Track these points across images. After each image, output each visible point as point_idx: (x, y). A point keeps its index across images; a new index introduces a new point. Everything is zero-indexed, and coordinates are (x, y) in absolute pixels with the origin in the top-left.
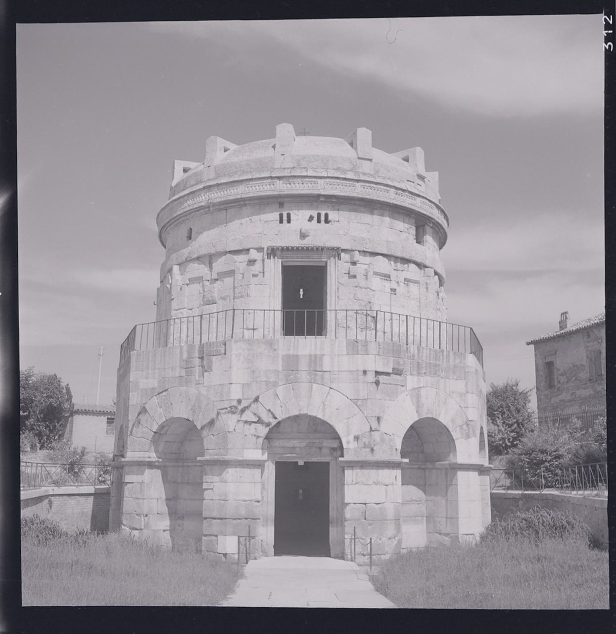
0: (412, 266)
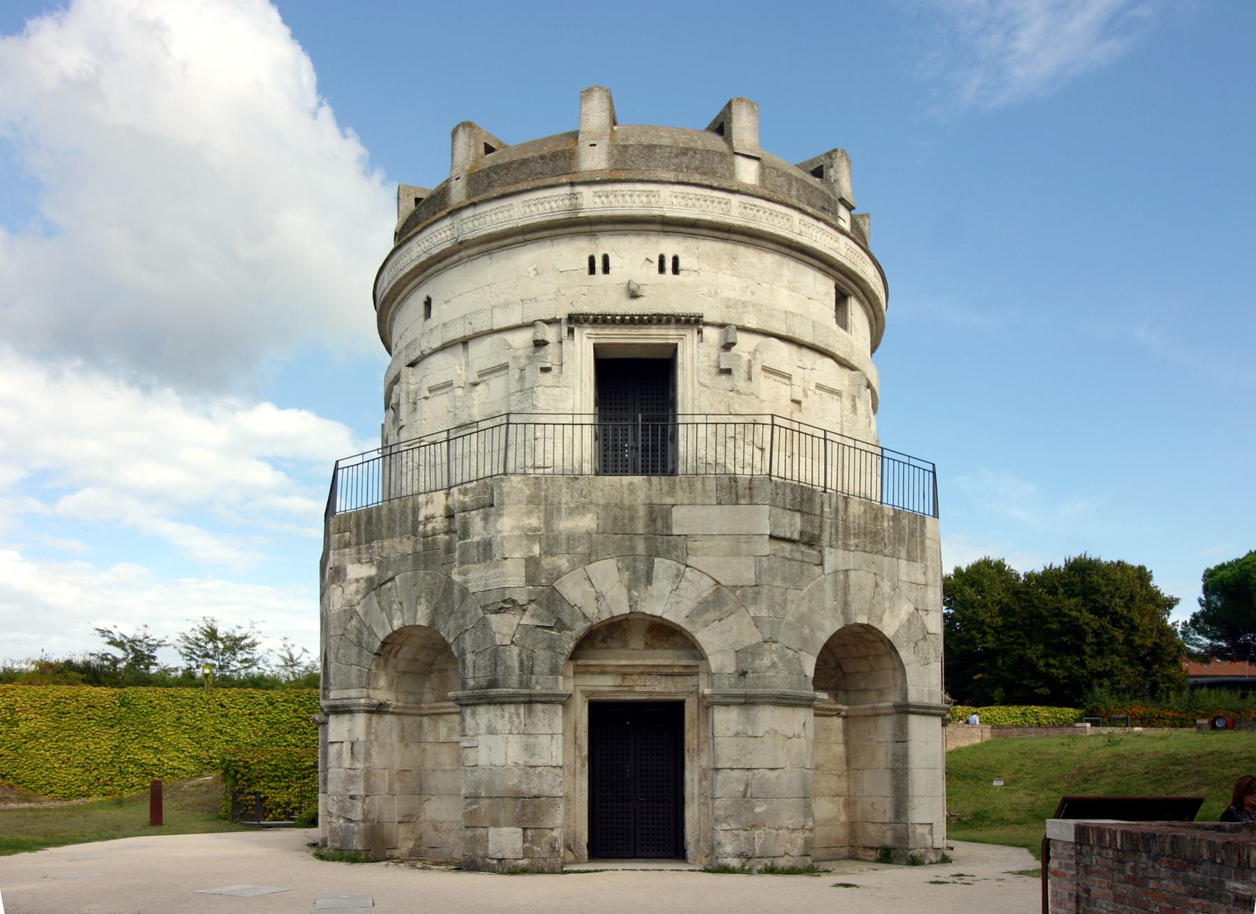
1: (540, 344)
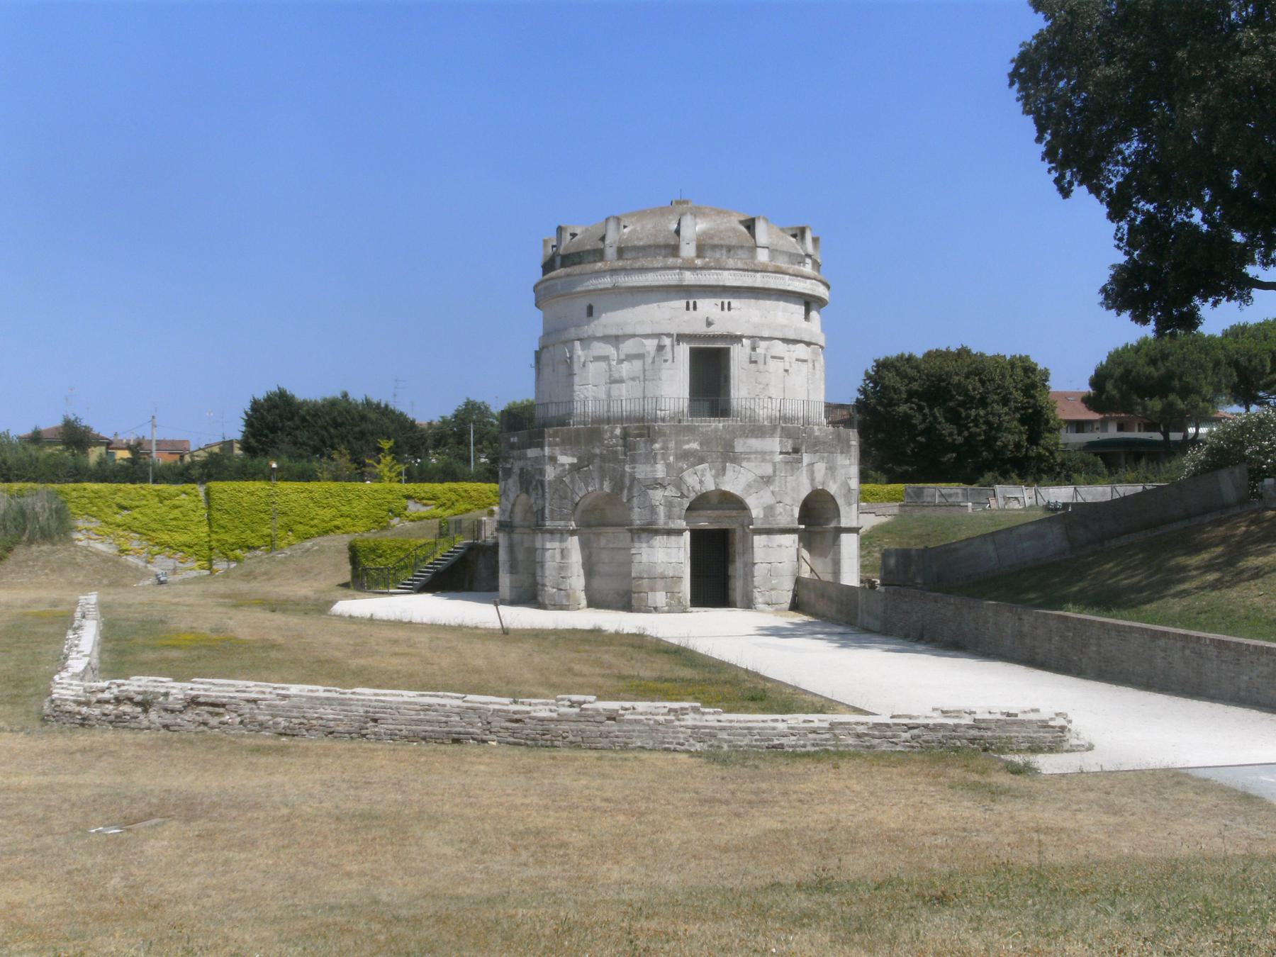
0: (802, 346)
1: (661, 348)
